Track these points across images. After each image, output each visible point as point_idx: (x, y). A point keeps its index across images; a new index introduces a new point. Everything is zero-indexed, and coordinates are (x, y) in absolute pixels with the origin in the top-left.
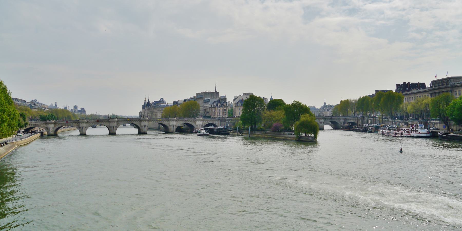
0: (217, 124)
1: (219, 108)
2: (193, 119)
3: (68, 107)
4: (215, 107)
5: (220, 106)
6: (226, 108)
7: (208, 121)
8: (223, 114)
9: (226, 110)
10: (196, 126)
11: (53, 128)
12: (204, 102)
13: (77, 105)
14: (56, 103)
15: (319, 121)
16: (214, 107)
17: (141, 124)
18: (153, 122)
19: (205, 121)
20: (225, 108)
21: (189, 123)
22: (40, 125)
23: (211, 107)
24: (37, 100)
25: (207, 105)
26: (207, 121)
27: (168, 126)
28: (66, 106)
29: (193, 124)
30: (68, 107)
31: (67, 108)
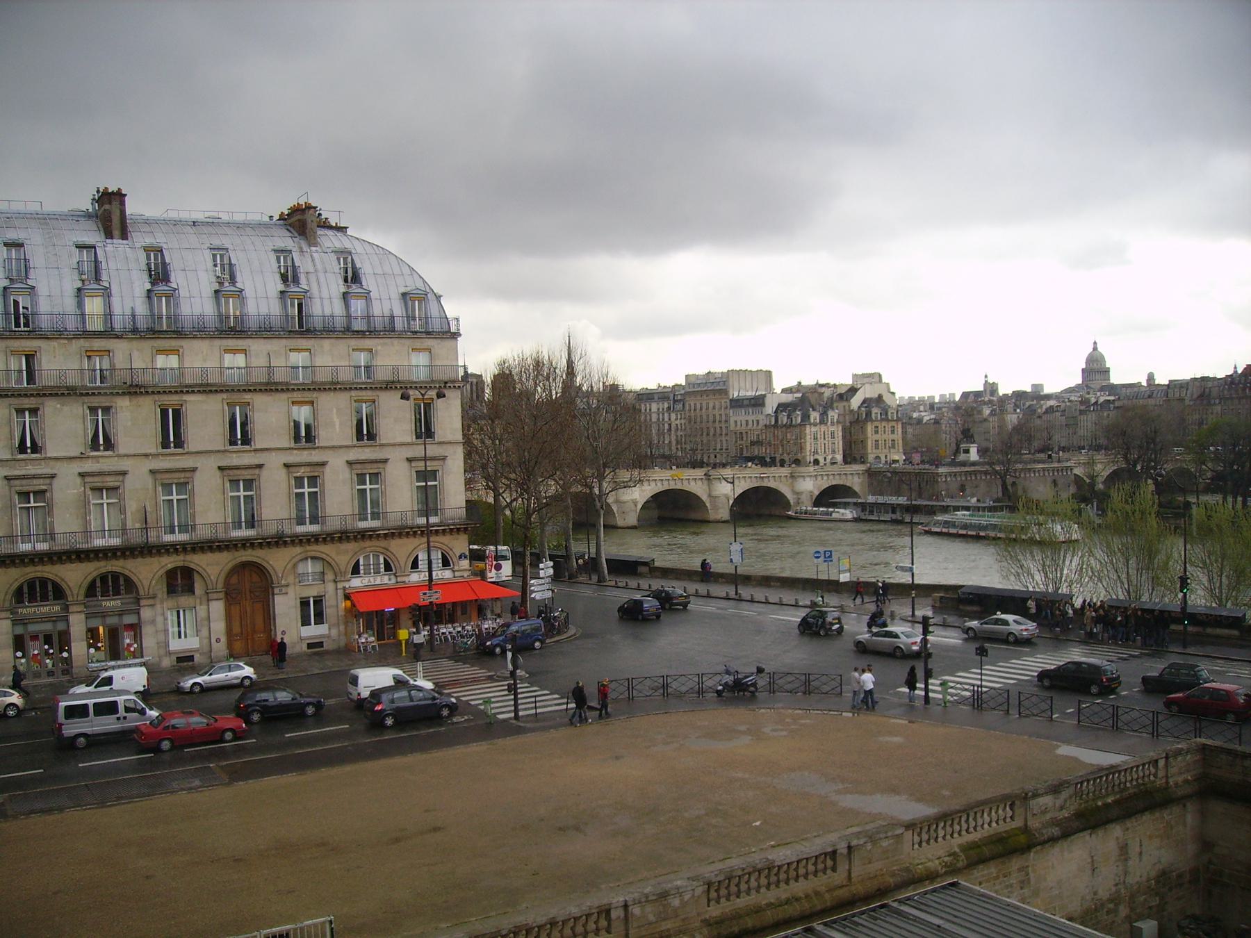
0: (857, 488)
1: (813, 429)
4: (800, 425)
5: (818, 421)
6: (835, 426)
8: (827, 450)
9: (836, 436)
10: (795, 496)
12: (732, 407)
16: (795, 426)
20: (832, 429)
21: (772, 484)
23: (773, 423)
25: (750, 418)
26: (825, 478)
27: (704, 498)
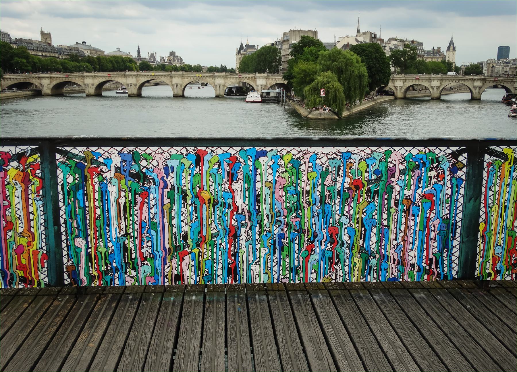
2: (251, 75)
3: (156, 53)
7: (275, 80)
11: (50, 84)
13: (174, 51)
14: (139, 47)
15: (473, 84)
17: (172, 82)
18: (189, 78)
19: (271, 80)
22: (31, 79)
24: (85, 42)
26: (274, 80)
28: (152, 52)
29: (252, 83)
30: (156, 53)
31: (155, 55)
